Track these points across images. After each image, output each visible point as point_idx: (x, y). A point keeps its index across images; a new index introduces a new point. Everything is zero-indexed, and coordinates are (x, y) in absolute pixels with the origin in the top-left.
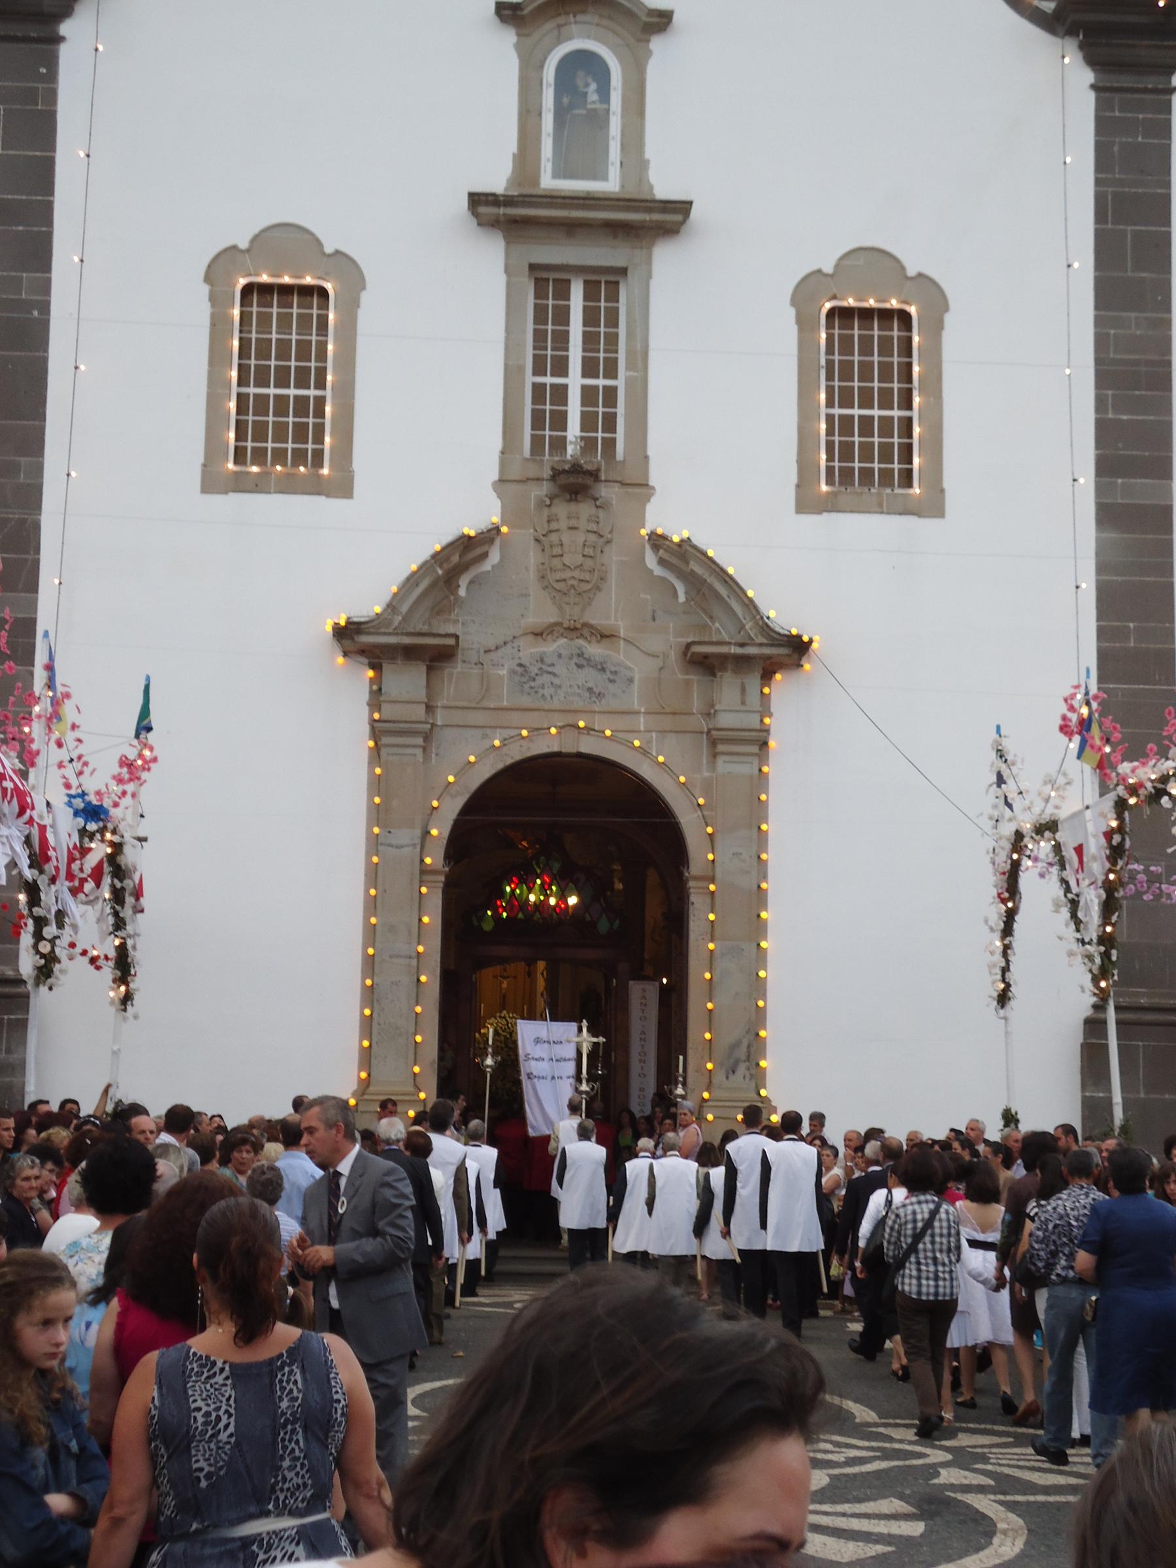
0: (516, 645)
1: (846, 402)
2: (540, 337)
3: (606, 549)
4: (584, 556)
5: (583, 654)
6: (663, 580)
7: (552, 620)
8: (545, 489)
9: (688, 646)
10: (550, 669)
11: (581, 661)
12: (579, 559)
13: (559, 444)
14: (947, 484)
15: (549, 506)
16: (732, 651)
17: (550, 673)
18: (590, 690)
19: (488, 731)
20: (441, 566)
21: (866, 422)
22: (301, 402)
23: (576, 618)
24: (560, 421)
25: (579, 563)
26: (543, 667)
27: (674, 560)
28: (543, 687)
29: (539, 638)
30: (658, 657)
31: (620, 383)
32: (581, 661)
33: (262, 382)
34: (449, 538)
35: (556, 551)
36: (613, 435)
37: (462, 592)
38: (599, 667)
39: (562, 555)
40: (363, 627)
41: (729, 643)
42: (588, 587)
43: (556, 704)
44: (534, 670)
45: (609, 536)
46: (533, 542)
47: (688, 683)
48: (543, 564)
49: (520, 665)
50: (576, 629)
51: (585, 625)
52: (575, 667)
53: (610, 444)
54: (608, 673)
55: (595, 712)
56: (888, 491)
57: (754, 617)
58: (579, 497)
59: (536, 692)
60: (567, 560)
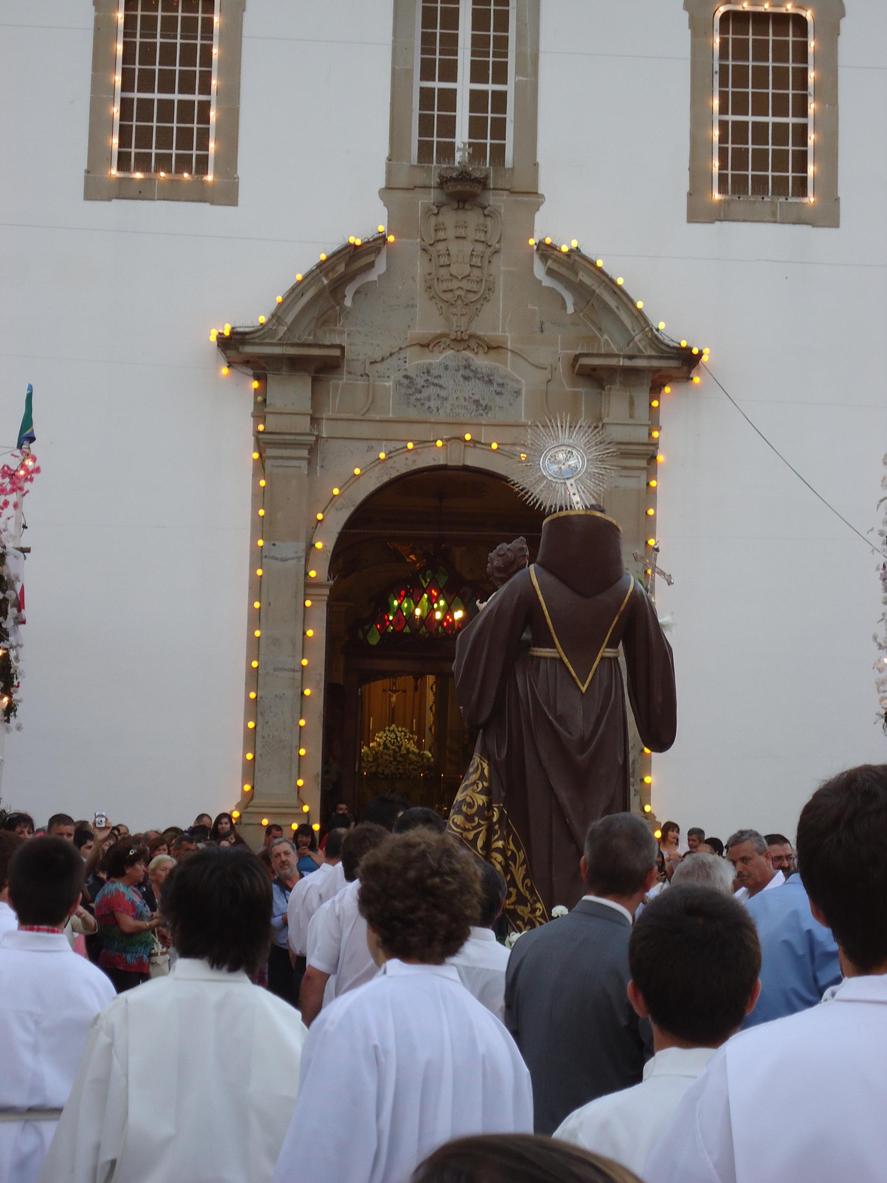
0: (402, 356)
1: (740, 107)
2: (427, 40)
3: (495, 260)
5: (469, 365)
6: (551, 290)
7: (439, 332)
8: (432, 197)
9: (577, 357)
10: (436, 381)
11: (468, 373)
12: (467, 270)
13: (447, 151)
14: (841, 193)
16: (621, 364)
18: (477, 402)
19: (373, 443)
20: (326, 276)
21: (760, 130)
22: (186, 107)
23: (463, 329)
24: (448, 126)
26: (430, 378)
27: (563, 271)
28: (429, 399)
29: (426, 350)
30: (546, 368)
31: (510, 88)
32: (468, 373)
33: (147, 86)
34: (335, 247)
35: (444, 260)
36: (503, 142)
37: (348, 302)
38: (486, 379)
39: (449, 265)
40: (247, 337)
41: (618, 356)
42: (475, 297)
43: (442, 417)
44: (420, 382)
47: (576, 396)
48: (430, 274)
49: (406, 377)
50: (462, 340)
51: (472, 336)
52: (462, 380)
53: (499, 152)
54: (495, 385)
55: (481, 425)
56: (782, 199)
57: (643, 330)
58: (467, 206)
59: (423, 404)
60: (453, 270)
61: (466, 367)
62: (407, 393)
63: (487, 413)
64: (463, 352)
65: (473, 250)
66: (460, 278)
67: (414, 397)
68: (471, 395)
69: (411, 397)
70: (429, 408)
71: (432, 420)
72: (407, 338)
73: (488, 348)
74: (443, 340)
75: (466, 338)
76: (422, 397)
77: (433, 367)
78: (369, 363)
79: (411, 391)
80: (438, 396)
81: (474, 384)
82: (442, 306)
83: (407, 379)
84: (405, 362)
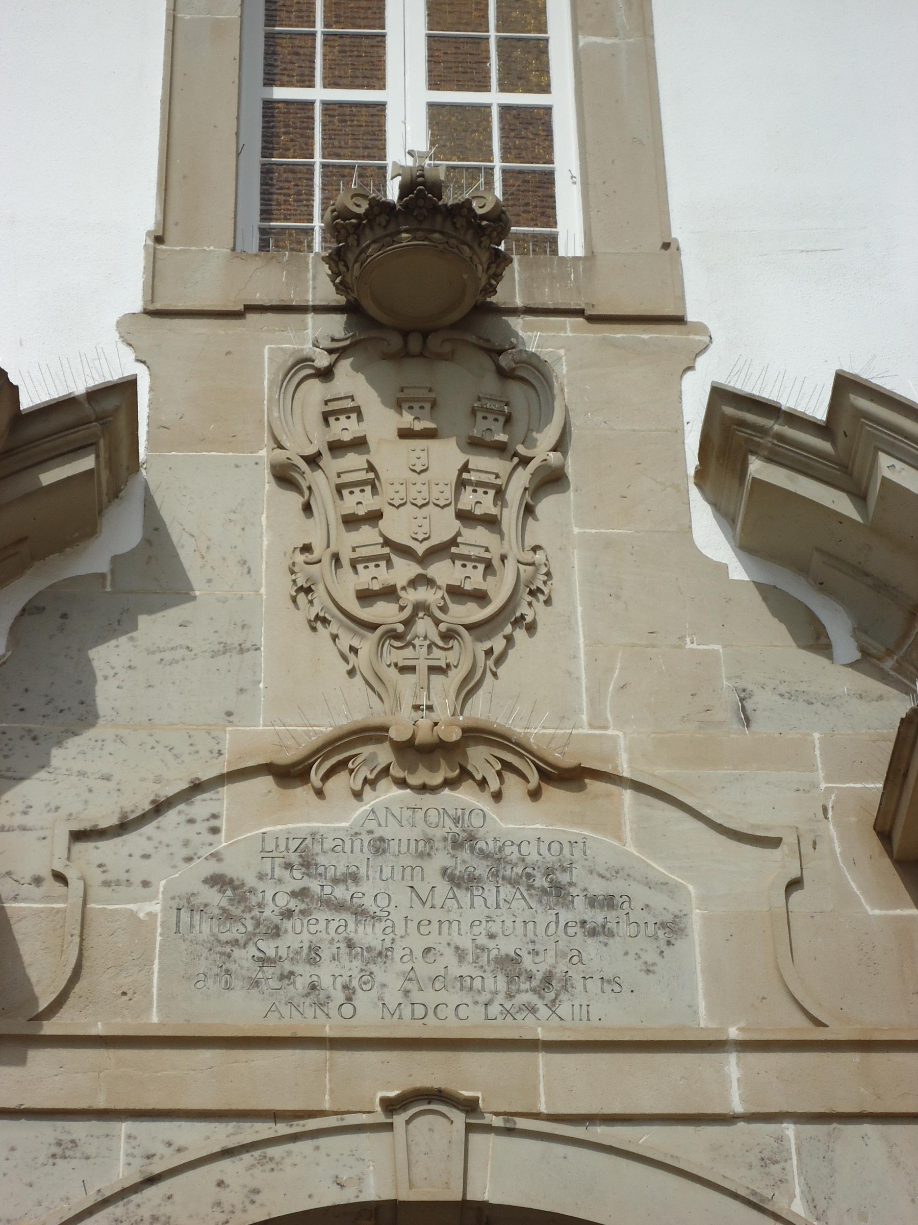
0: (201, 806)
3: (546, 506)
4: (464, 517)
5: (472, 838)
10: (340, 893)
15: (326, 374)
17: (340, 907)
19: (79, 1129)
25: (447, 537)
26: (314, 886)
28: (313, 955)
29: (302, 793)
30: (774, 843)
38: (541, 881)
39: (374, 517)
45: (554, 458)
46: (268, 484)
48: (306, 548)
49: (217, 881)
52: (443, 887)
54: (579, 902)
55: (533, 1045)
58: (434, 342)
61: (457, 845)
62: (224, 937)
63: (552, 1005)
64: (447, 791)
65: (465, 468)
66: (420, 549)
67: (252, 950)
68: (483, 940)
69: (237, 953)
70: (313, 987)
71: (328, 1032)
72: (220, 753)
73: (545, 776)
74: (365, 751)
75: (455, 735)
76: (283, 952)
77: (329, 844)
78: (66, 836)
79: (236, 931)
80: (350, 944)
81: (491, 901)
82: (355, 643)
83: (222, 891)
84: (215, 831)
